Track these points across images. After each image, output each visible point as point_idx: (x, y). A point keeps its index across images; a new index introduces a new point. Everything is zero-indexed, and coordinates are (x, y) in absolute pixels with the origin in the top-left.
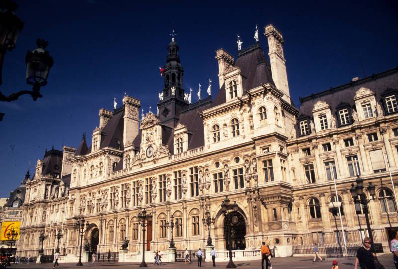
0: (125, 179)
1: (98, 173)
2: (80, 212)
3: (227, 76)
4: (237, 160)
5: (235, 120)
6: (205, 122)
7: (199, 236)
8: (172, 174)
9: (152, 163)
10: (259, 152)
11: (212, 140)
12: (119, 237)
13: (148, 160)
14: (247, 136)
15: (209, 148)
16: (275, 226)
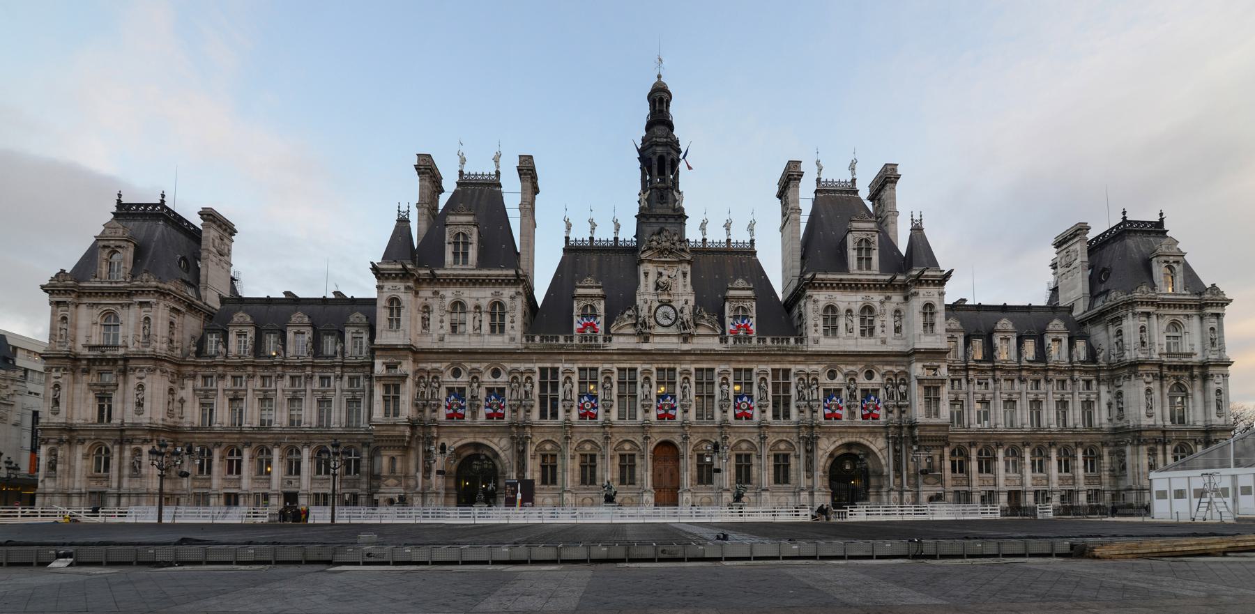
0: (590, 357)
1: (486, 327)
2: (421, 411)
3: (855, 225)
4: (870, 375)
5: (868, 309)
6: (808, 293)
7: (788, 486)
8: (732, 371)
9: (675, 340)
10: (917, 369)
11: (821, 328)
12: (577, 479)
13: (659, 330)
14: (885, 340)
15: (816, 342)
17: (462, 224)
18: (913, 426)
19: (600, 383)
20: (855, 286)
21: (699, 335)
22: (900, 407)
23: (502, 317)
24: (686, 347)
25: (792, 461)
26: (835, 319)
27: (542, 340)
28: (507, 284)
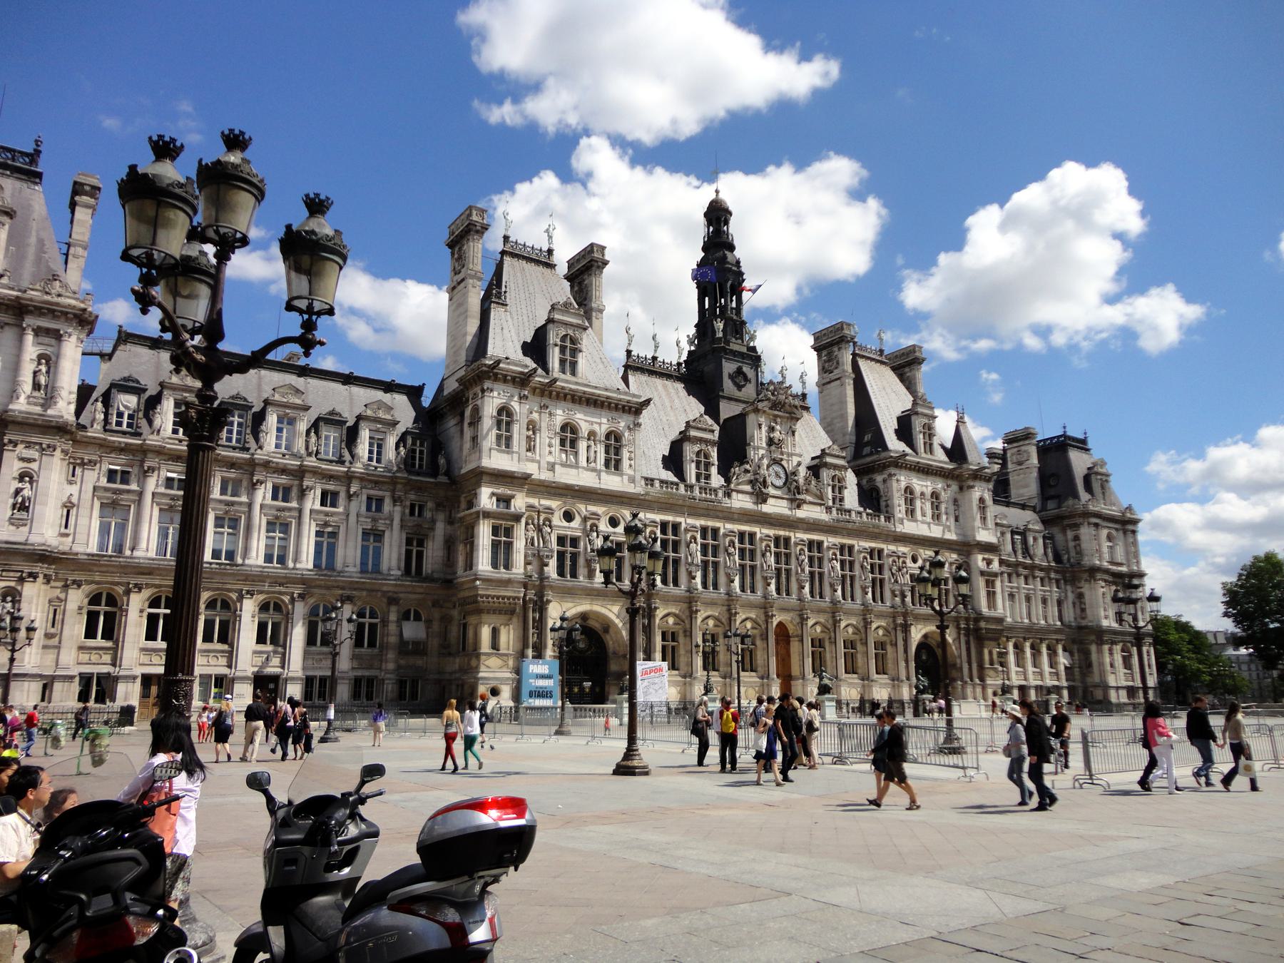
5: (935, 495)
10: (979, 560)
11: (903, 508)
15: (902, 523)
16: (991, 673)
17: (572, 325)
18: (979, 617)
19: (722, 546)
20: (925, 471)
21: (811, 503)
22: (964, 596)
23: (618, 451)
24: (801, 514)
25: (889, 648)
26: (911, 500)
27: (662, 487)
28: (624, 411)
